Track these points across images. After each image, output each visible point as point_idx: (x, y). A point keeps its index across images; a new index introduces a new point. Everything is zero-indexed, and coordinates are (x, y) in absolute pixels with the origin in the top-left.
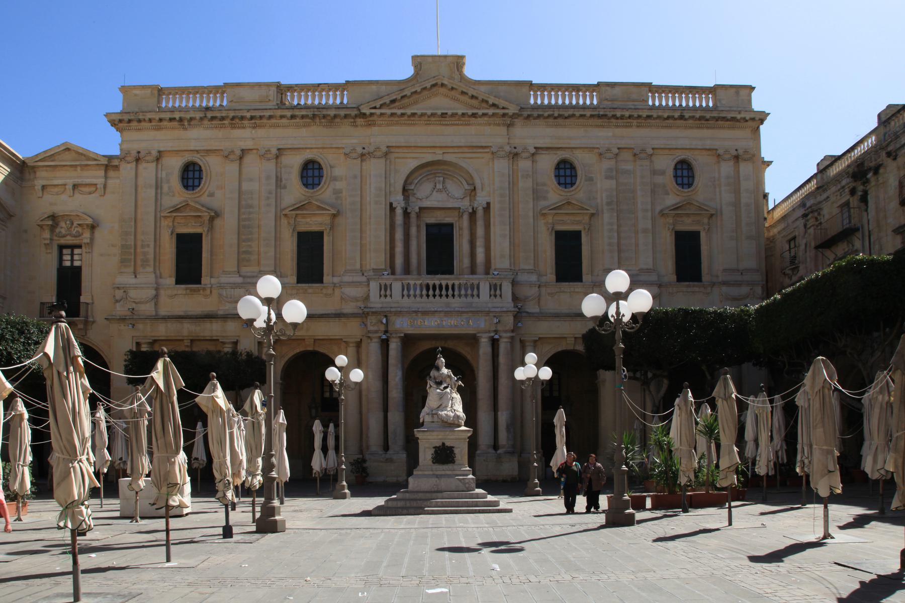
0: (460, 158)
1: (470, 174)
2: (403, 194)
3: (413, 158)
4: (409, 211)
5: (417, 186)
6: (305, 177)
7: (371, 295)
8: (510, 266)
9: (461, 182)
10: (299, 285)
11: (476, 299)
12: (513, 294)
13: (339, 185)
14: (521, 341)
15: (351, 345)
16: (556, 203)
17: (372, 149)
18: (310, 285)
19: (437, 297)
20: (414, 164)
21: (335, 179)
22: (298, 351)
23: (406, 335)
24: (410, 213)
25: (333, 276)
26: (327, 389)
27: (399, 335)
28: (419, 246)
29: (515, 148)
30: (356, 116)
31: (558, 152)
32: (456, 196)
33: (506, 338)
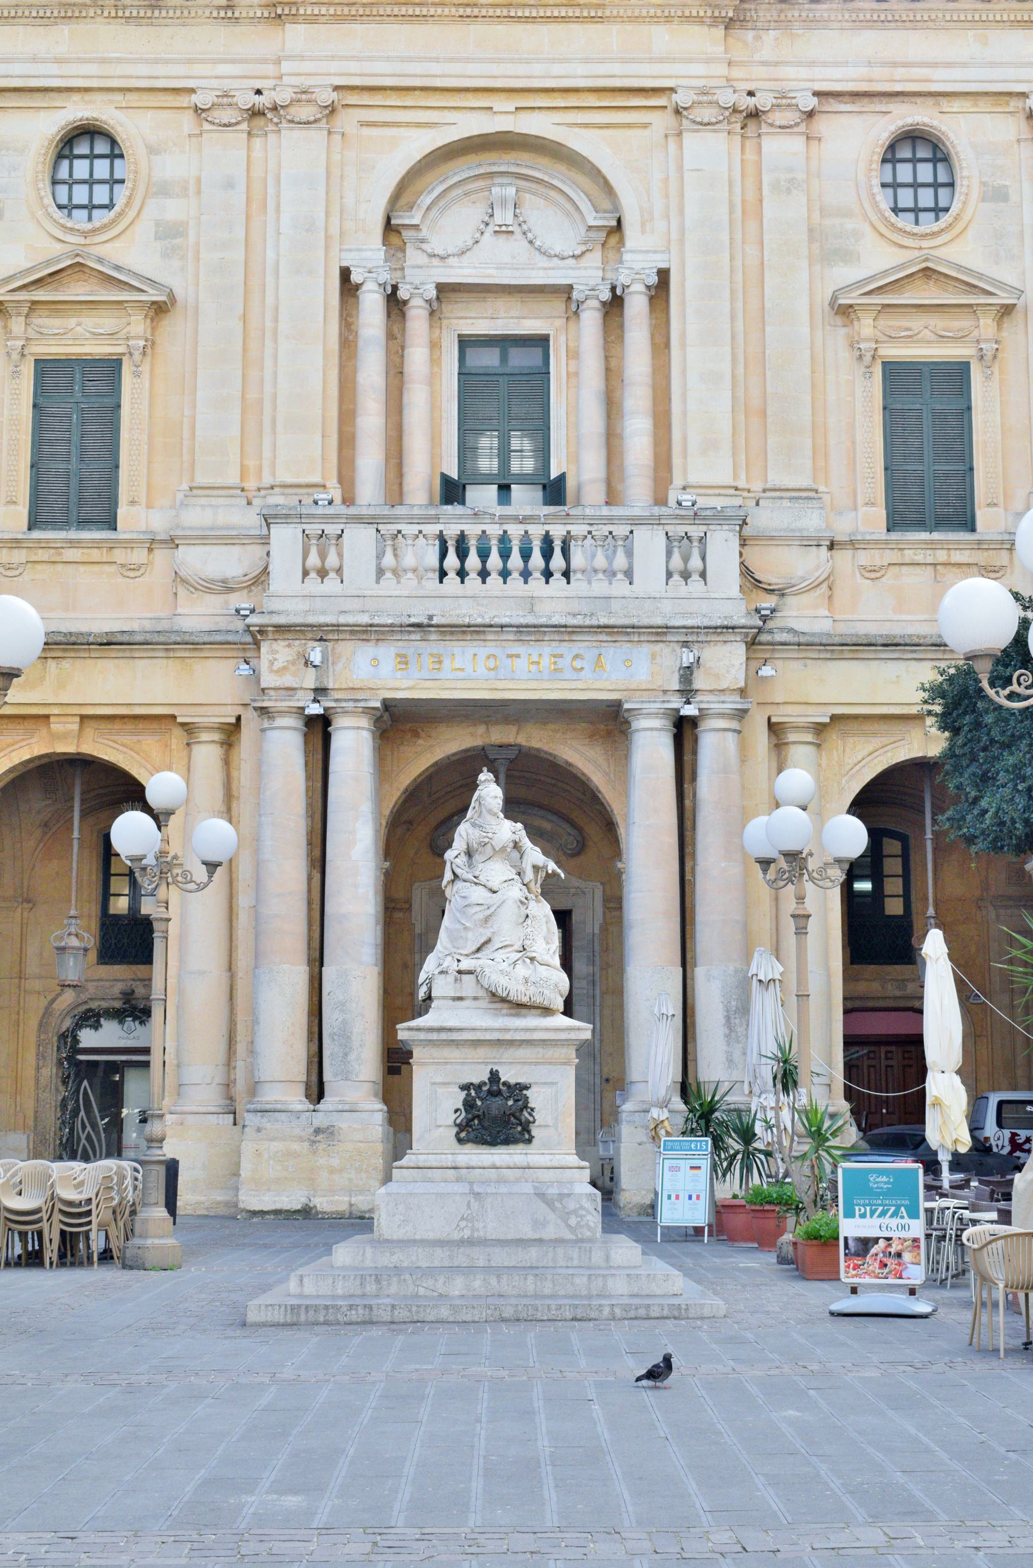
0: (569, 125)
1: (605, 178)
2: (385, 241)
3: (419, 125)
4: (403, 294)
5: (433, 213)
6: (64, 182)
7: (271, 568)
8: (735, 476)
9: (577, 208)
10: (36, 534)
11: (620, 587)
12: (746, 572)
13: (173, 210)
14: (774, 728)
15: (204, 736)
16: (885, 273)
17: (283, 96)
18: (73, 534)
19: (494, 579)
21: (164, 190)
22: (27, 757)
23: (388, 705)
24: (405, 302)
25: (149, 506)
26: (118, 885)
27: (362, 704)
28: (434, 406)
29: (751, 94)
31: (891, 107)
32: (557, 250)
33: (722, 715)
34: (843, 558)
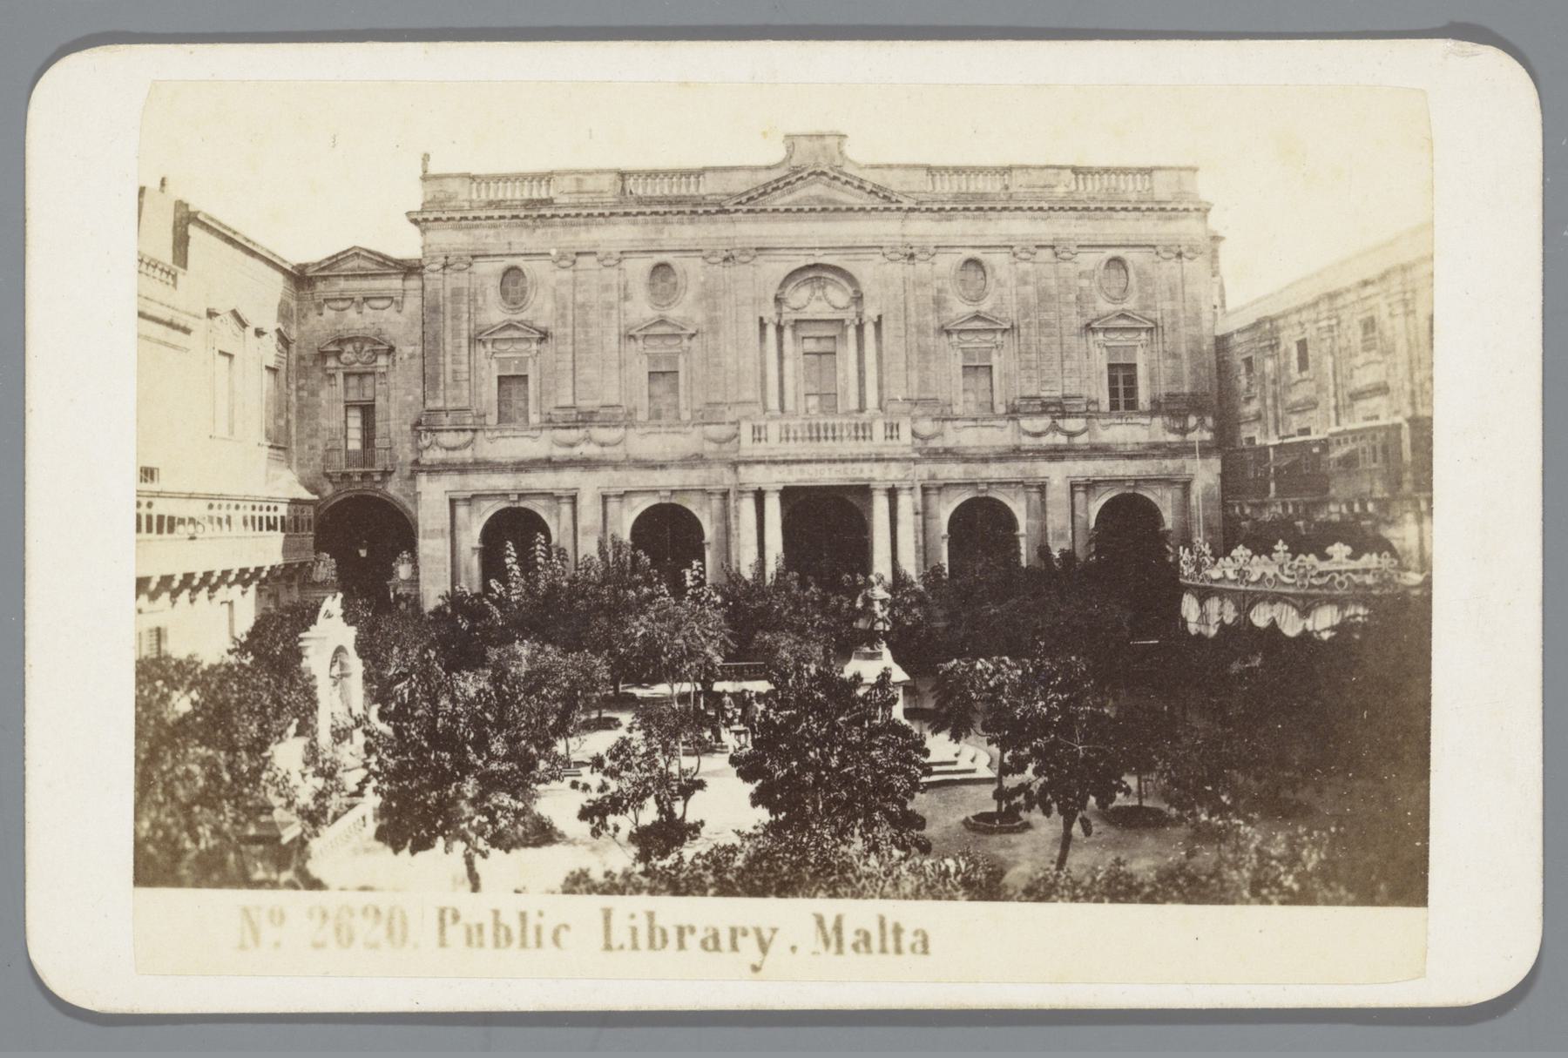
20: (784, 269)
30: (717, 212)
34: (948, 424)
